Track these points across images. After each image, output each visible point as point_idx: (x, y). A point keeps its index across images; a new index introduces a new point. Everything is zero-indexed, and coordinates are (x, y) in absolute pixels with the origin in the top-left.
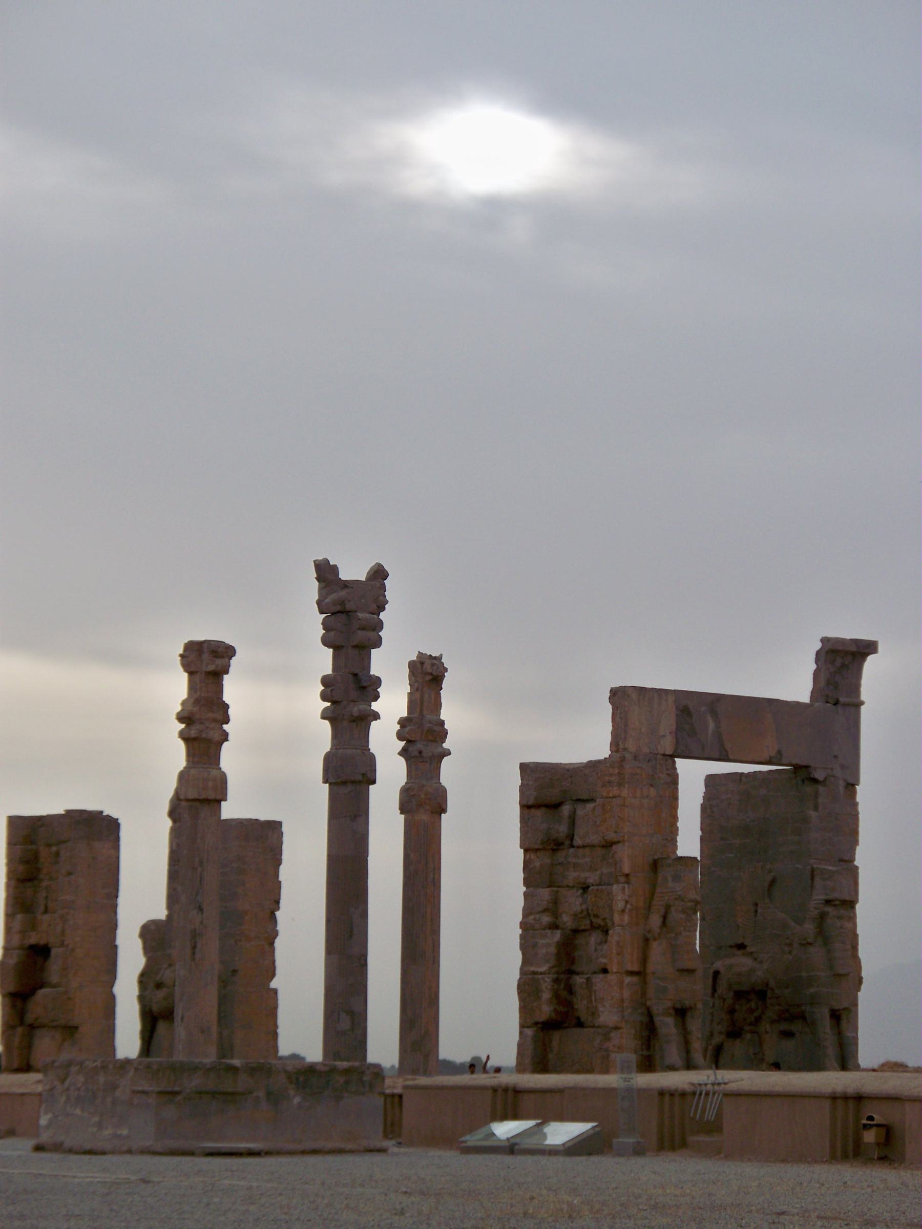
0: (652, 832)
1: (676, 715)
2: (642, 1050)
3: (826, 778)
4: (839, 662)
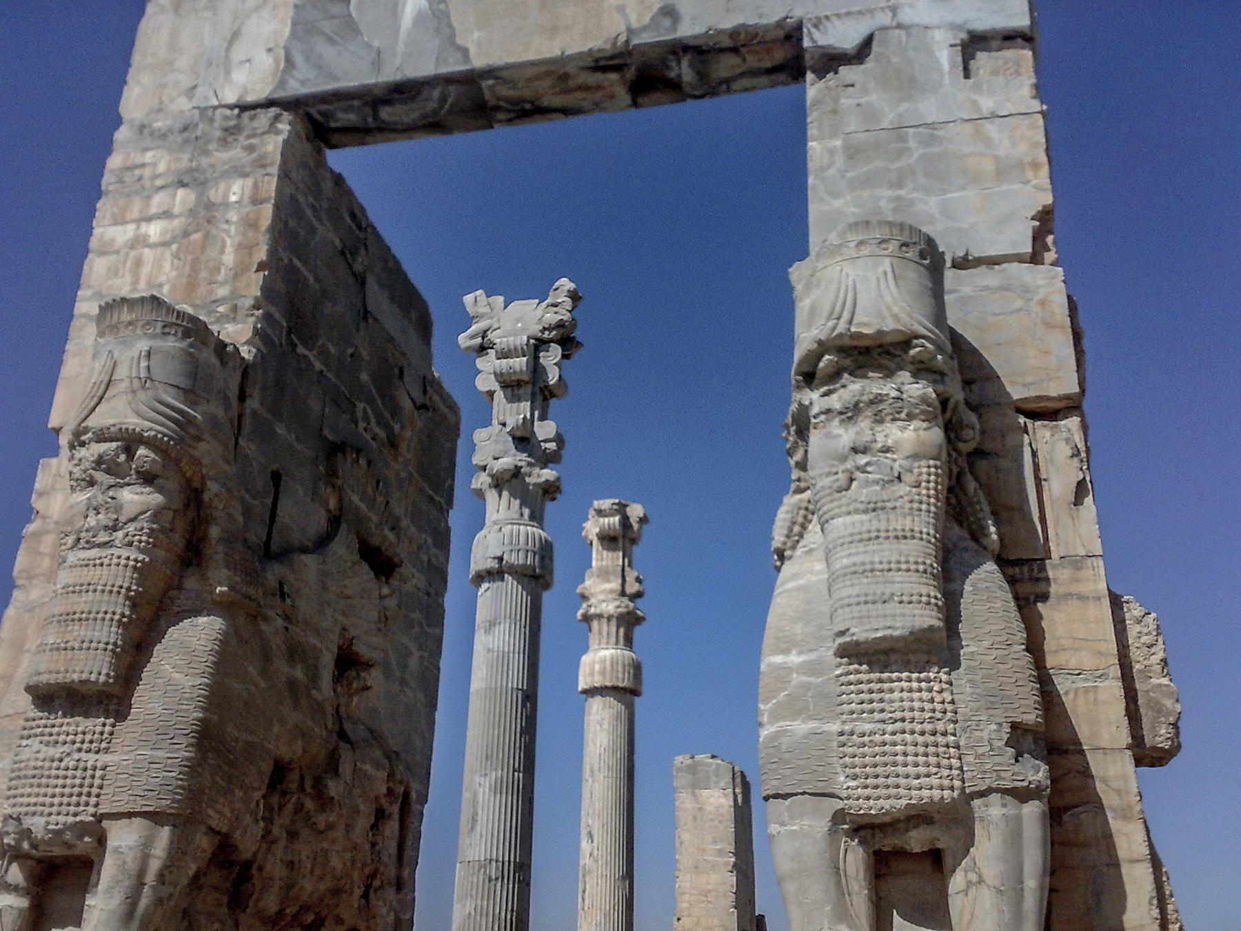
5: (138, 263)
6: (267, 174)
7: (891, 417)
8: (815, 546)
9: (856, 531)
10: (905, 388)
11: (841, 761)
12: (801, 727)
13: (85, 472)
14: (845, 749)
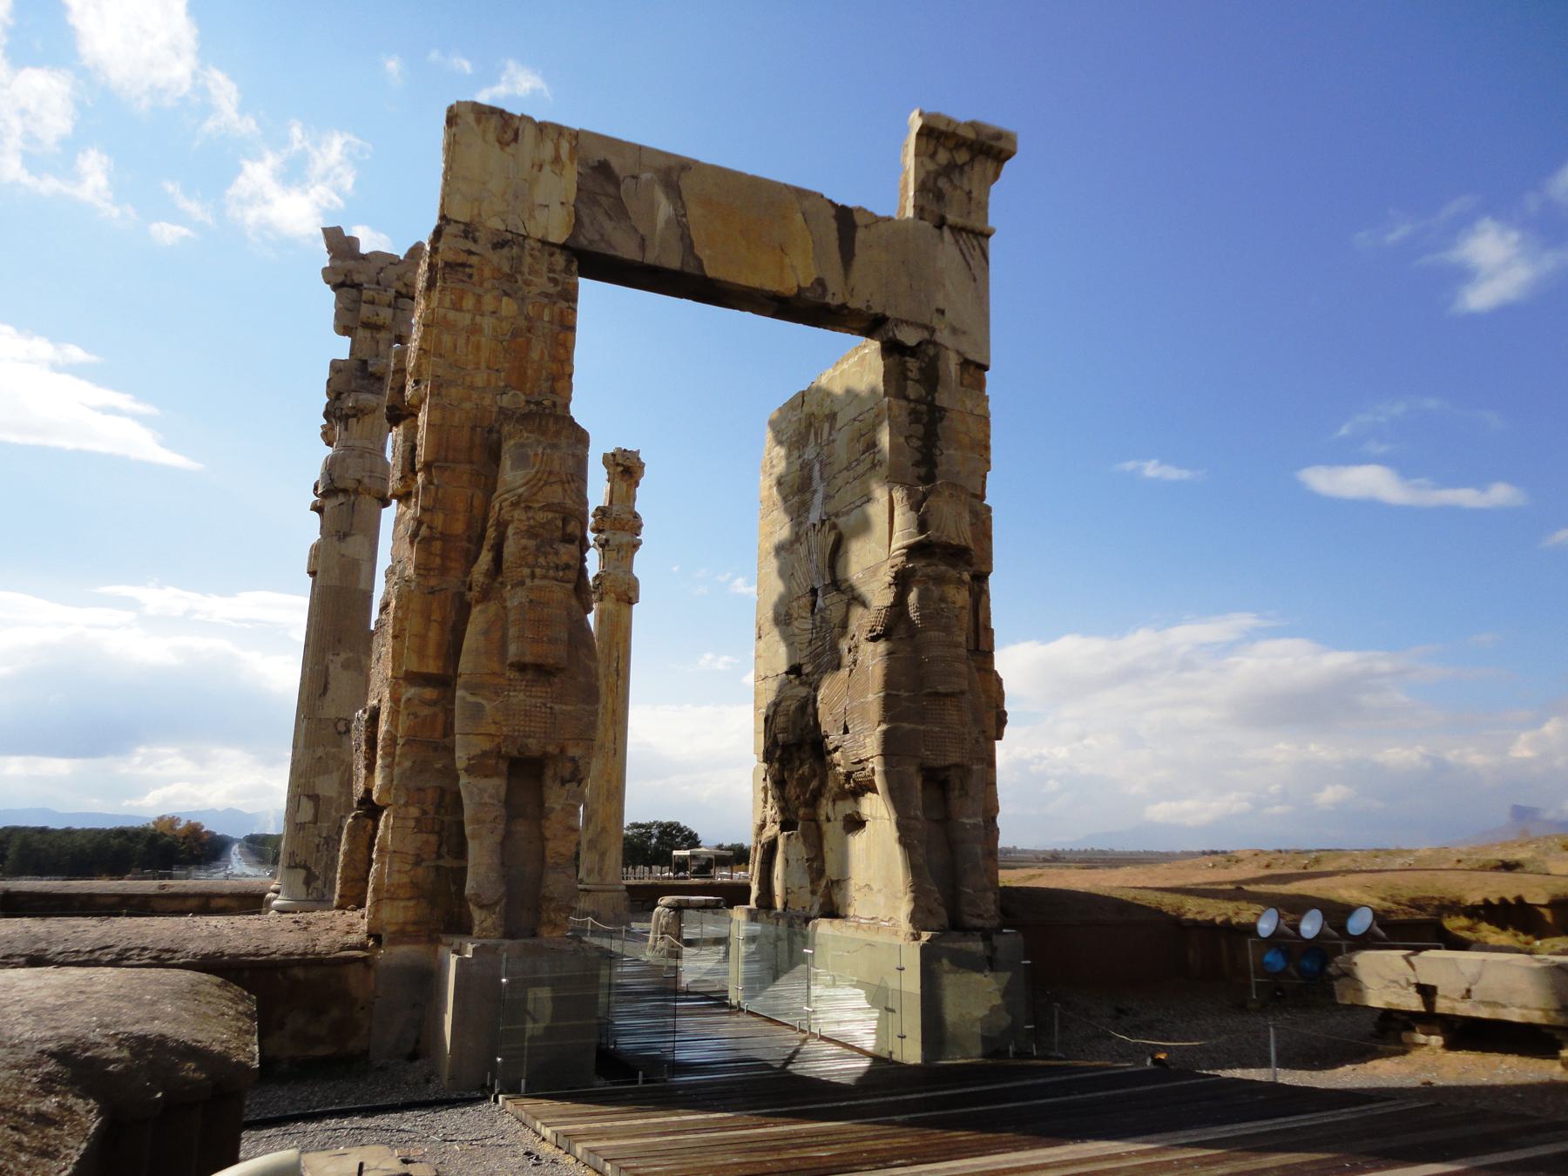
0: (502, 384)
1: (578, 173)
2: (439, 856)
3: (920, 344)
4: (943, 157)
5: (478, 347)
6: (570, 307)
13: (532, 527)
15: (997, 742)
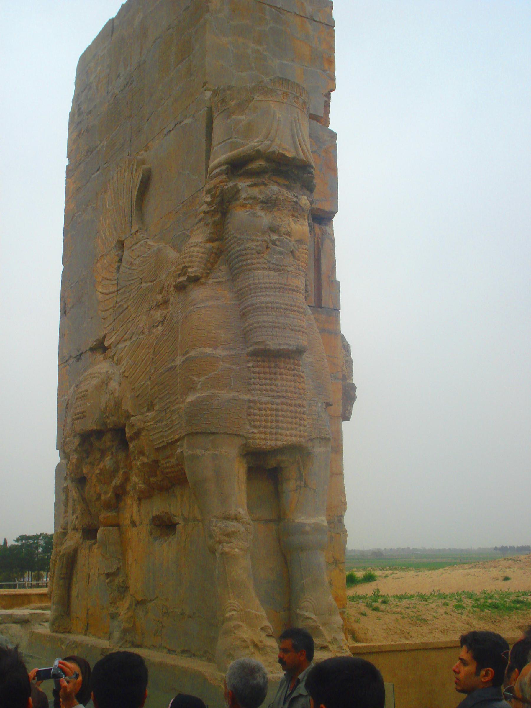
7: (291, 213)
8: (223, 280)
9: (271, 281)
10: (300, 197)
11: (249, 417)
12: (226, 395)
14: (252, 411)
15: (344, 424)
